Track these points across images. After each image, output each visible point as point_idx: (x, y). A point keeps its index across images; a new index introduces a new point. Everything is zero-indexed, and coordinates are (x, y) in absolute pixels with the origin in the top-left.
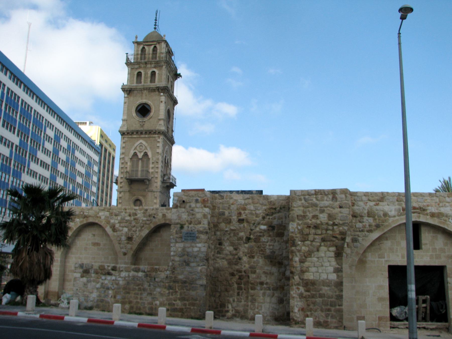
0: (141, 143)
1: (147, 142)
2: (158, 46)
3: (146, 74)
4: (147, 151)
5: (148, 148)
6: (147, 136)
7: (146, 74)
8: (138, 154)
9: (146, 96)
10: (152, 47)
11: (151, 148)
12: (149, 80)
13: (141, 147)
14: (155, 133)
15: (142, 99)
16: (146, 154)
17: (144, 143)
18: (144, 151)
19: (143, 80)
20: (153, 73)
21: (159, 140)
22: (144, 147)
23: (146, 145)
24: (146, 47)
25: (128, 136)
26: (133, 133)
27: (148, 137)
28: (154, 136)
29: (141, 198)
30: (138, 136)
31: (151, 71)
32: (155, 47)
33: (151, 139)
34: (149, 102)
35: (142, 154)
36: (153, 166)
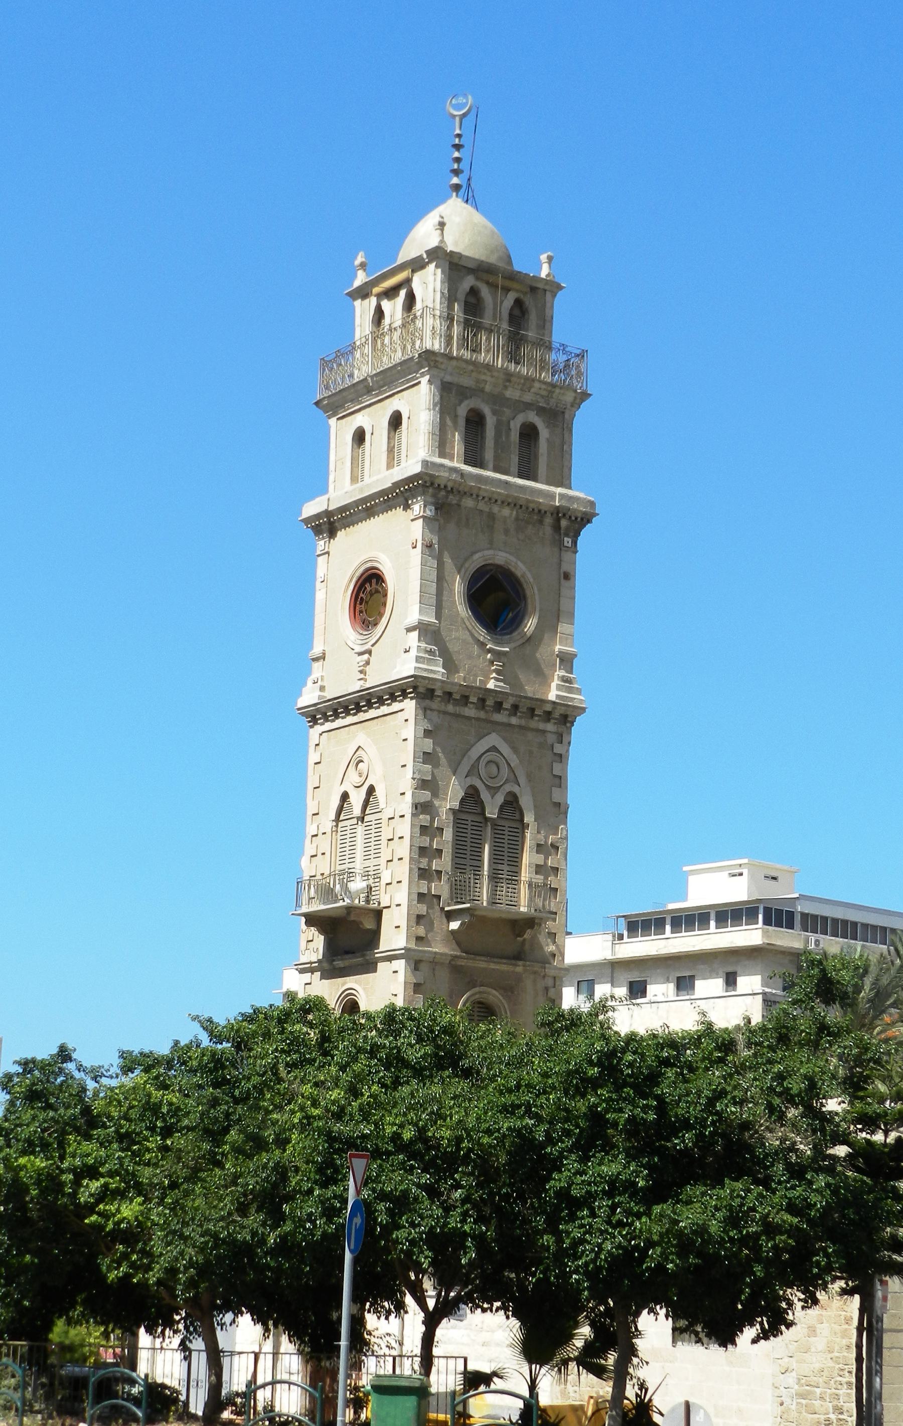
0: (494, 749)
1: (515, 750)
2: (528, 301)
3: (502, 428)
4: (516, 789)
5: (522, 780)
6: (514, 721)
7: (502, 428)
8: (485, 795)
9: (506, 532)
10: (511, 297)
11: (530, 777)
12: (515, 459)
13: (494, 769)
14: (548, 716)
15: (491, 545)
16: (512, 804)
17: (505, 749)
18: (508, 788)
19: (489, 455)
20: (529, 434)
21: (558, 749)
22: (505, 771)
23: (514, 761)
24: (485, 292)
25: (443, 707)
26: (465, 700)
27: (520, 727)
28: (541, 726)
29: (494, 996)
30: (482, 715)
31: (520, 419)
32: (518, 303)
33: (530, 736)
34: (520, 569)
35: (500, 799)
36: (540, 859)
